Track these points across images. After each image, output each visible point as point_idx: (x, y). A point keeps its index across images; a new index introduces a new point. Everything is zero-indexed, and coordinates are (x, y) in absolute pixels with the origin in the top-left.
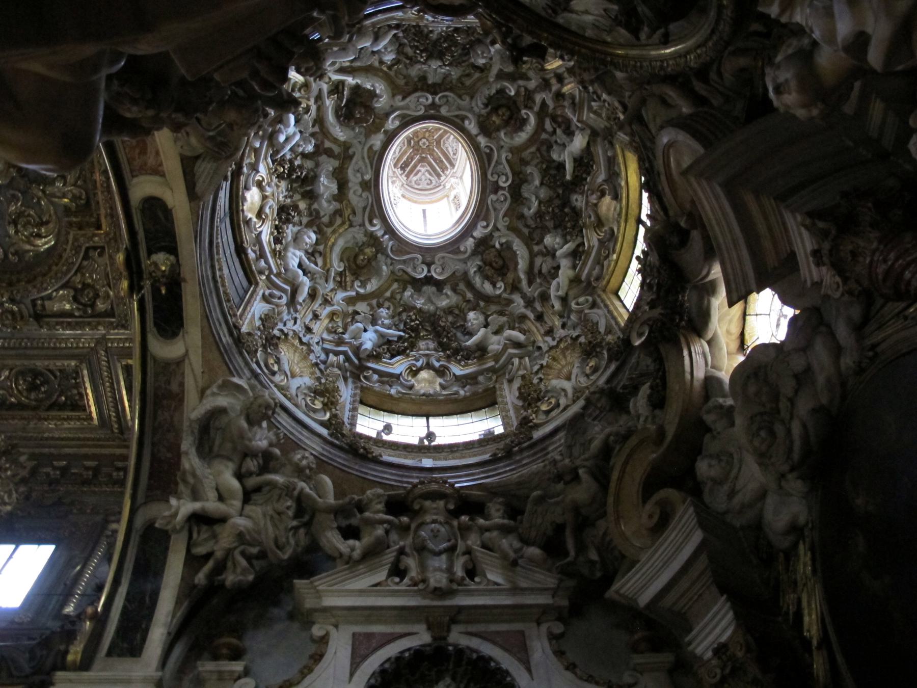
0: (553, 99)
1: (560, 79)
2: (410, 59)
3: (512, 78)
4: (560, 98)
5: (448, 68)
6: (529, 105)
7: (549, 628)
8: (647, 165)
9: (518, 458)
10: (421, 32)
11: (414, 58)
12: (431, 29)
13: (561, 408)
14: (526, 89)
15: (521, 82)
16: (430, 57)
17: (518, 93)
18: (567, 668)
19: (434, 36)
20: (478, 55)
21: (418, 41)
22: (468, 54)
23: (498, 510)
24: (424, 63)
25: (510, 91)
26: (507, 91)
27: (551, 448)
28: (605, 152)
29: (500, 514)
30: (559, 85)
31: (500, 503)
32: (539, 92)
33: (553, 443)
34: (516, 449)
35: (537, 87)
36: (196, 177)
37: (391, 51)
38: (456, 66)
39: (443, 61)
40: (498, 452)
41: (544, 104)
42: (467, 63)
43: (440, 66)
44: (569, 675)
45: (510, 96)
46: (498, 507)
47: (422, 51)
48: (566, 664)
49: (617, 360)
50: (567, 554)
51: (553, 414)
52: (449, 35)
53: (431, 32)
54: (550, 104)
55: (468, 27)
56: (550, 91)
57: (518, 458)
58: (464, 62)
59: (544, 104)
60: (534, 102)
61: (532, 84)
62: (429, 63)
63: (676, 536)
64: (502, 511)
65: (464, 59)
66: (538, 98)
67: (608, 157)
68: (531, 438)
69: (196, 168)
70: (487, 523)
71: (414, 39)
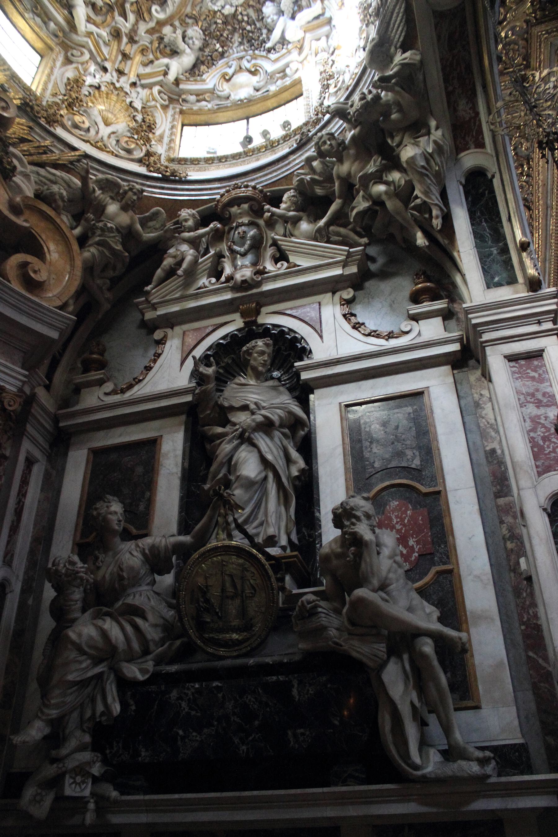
0: (120, 29)
1: (126, 57)
2: (249, 6)
3: (161, 24)
4: (115, 34)
5: (216, 9)
6: (135, 5)
8: (43, 122)
10: (249, 41)
11: (247, 7)
12: (242, 47)
14: (145, 20)
15: (152, 24)
16: (234, 15)
17: (150, 12)
19: (237, 38)
20: (196, 39)
21: (249, 31)
22: (204, 31)
24: (236, 7)
25: (156, 11)
26: (159, 9)
28: (57, 23)
30: (122, 48)
32: (133, 26)
35: (138, 28)
36: (404, 20)
37: (268, 17)
38: (209, 11)
39: (223, 14)
41: (124, 15)
42: (202, 18)
43: (223, 7)
45: (154, 3)
47: (243, 20)
52: (226, 45)
53: (241, 43)
54: (120, 19)
55: (213, 64)
56: (126, 35)
58: (205, 19)
59: (124, 15)
60: (133, 12)
61: (143, 28)
62: (233, 10)
65: (205, 25)
66: (132, 17)
67: (50, 19)
69: (405, 29)
71: (253, 32)
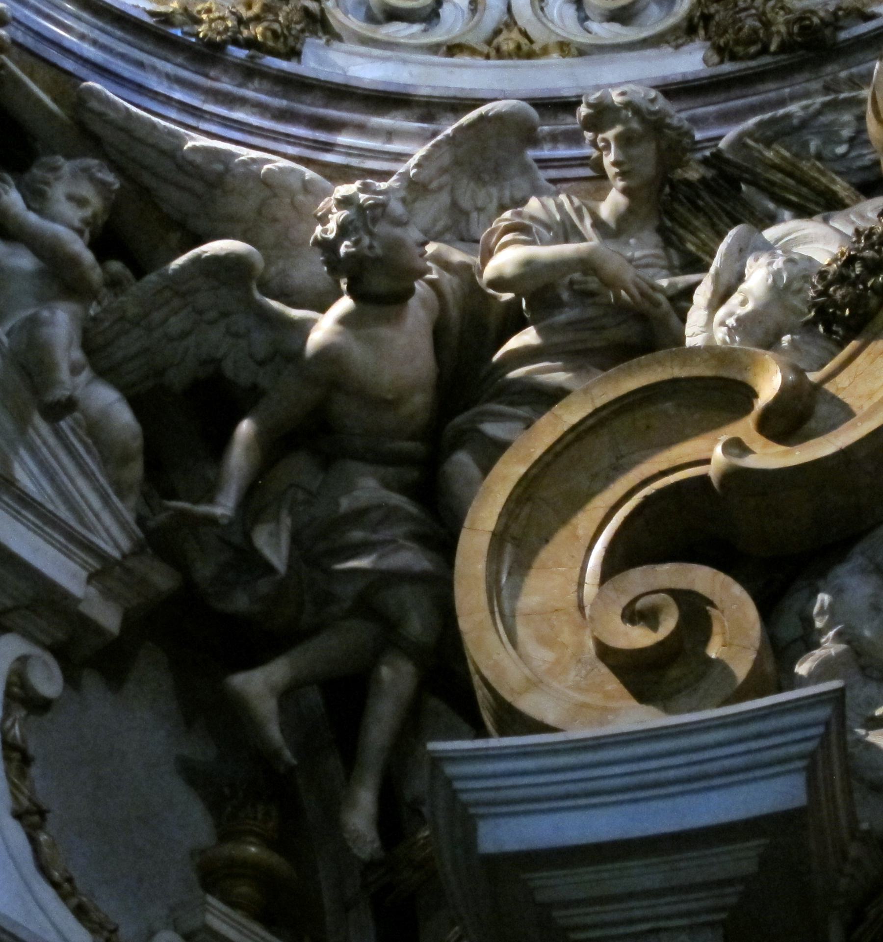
7: (23, 660)
9: (226, 85)
13: (439, 35)
18: (18, 816)
23: (81, 202)
27: (344, 139)
29: (75, 214)
31: (101, 186)
33: (361, 129)
34: (241, 53)
40: (179, 18)
44: (16, 834)
46: (86, 190)
48: (26, 803)
49: (723, 52)
50: (210, 494)
51: (399, 31)
57: (226, 85)
63: (720, 745)
64: (88, 212)
68: (294, 54)
70: (33, 218)
